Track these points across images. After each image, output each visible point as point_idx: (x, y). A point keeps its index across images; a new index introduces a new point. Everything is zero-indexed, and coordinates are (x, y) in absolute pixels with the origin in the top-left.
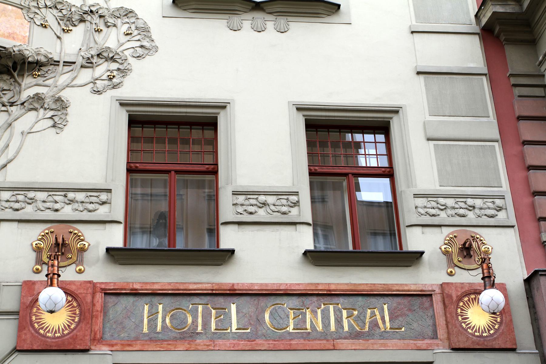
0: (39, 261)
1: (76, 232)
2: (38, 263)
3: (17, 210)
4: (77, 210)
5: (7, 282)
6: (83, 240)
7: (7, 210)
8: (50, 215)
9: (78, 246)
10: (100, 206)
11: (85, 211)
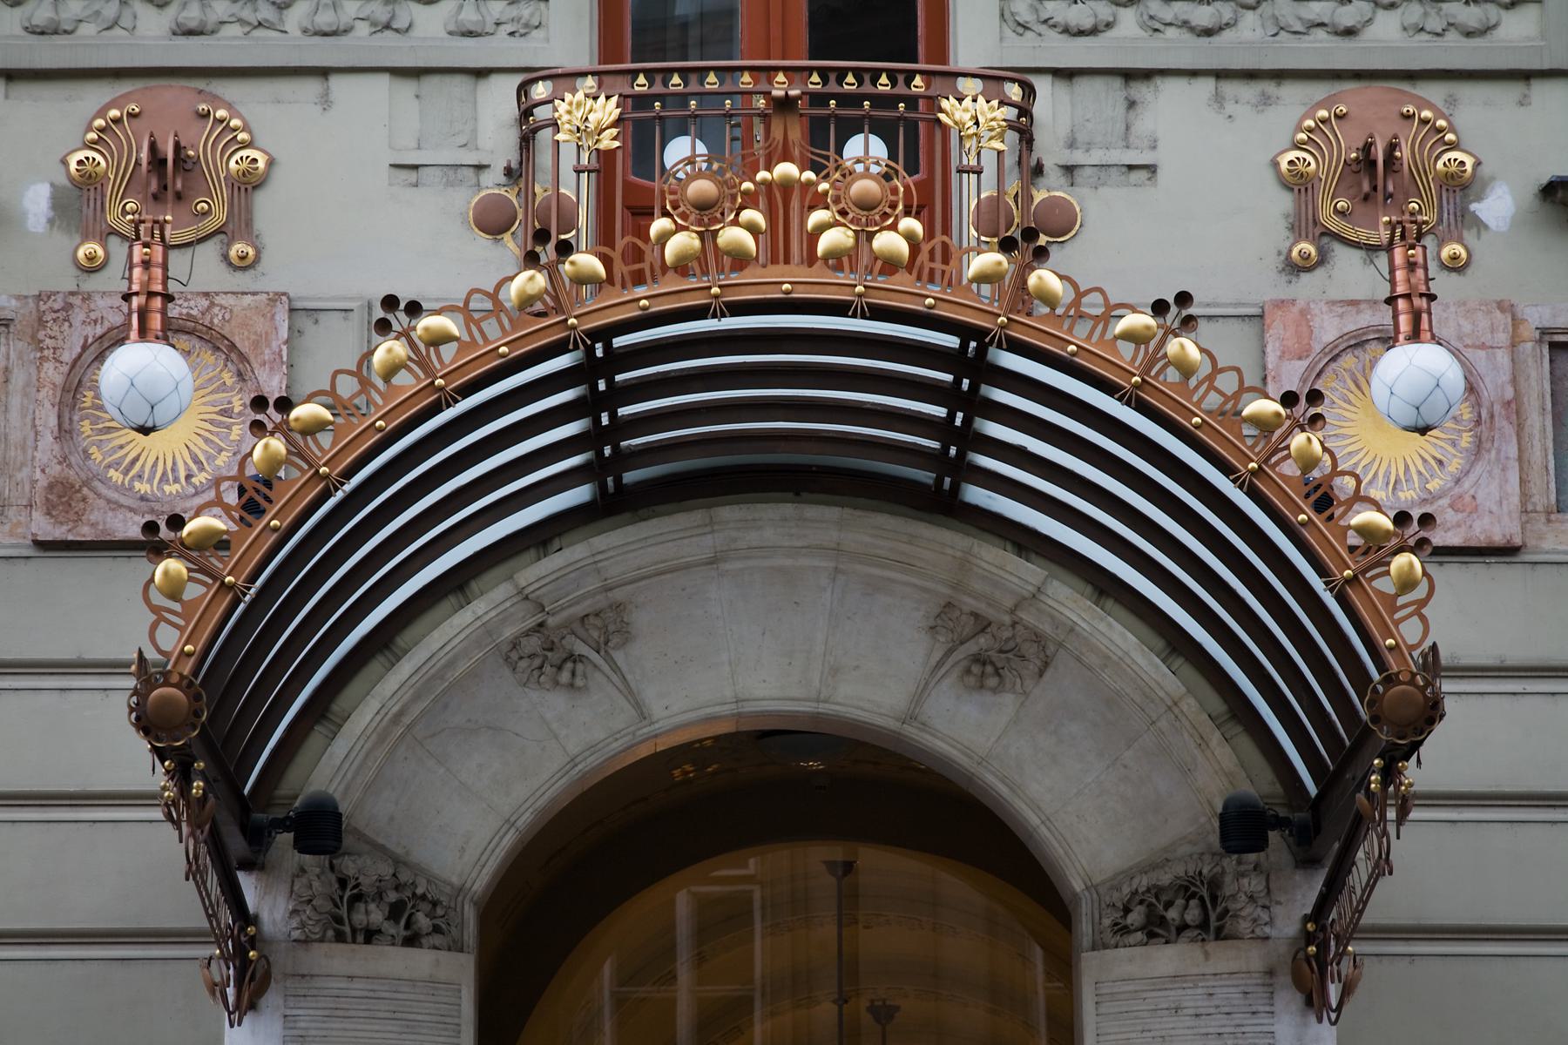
0: (1305, 224)
1: (1426, 114)
2: (1303, 233)
3: (1208, 32)
4: (1422, 29)
5: (1208, 305)
6: (1453, 146)
7: (1171, 32)
8: (1322, 51)
9: (1440, 165)
10: (1503, 13)
11: (1452, 36)
